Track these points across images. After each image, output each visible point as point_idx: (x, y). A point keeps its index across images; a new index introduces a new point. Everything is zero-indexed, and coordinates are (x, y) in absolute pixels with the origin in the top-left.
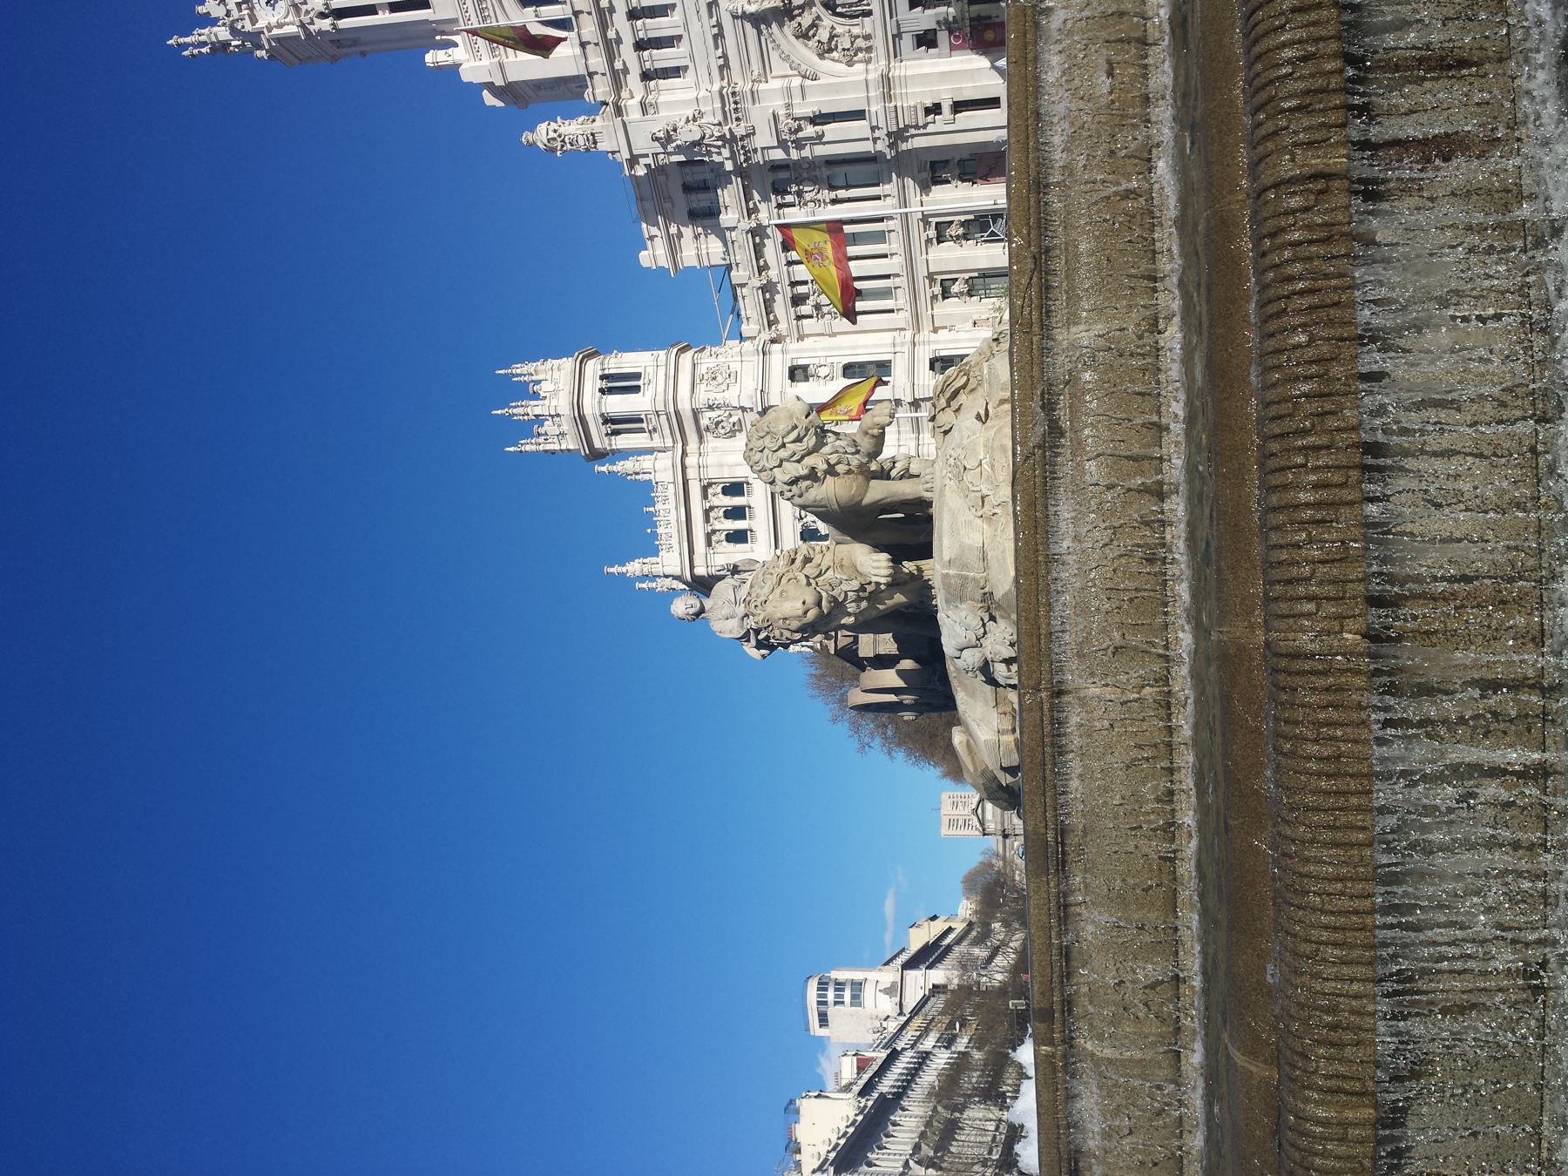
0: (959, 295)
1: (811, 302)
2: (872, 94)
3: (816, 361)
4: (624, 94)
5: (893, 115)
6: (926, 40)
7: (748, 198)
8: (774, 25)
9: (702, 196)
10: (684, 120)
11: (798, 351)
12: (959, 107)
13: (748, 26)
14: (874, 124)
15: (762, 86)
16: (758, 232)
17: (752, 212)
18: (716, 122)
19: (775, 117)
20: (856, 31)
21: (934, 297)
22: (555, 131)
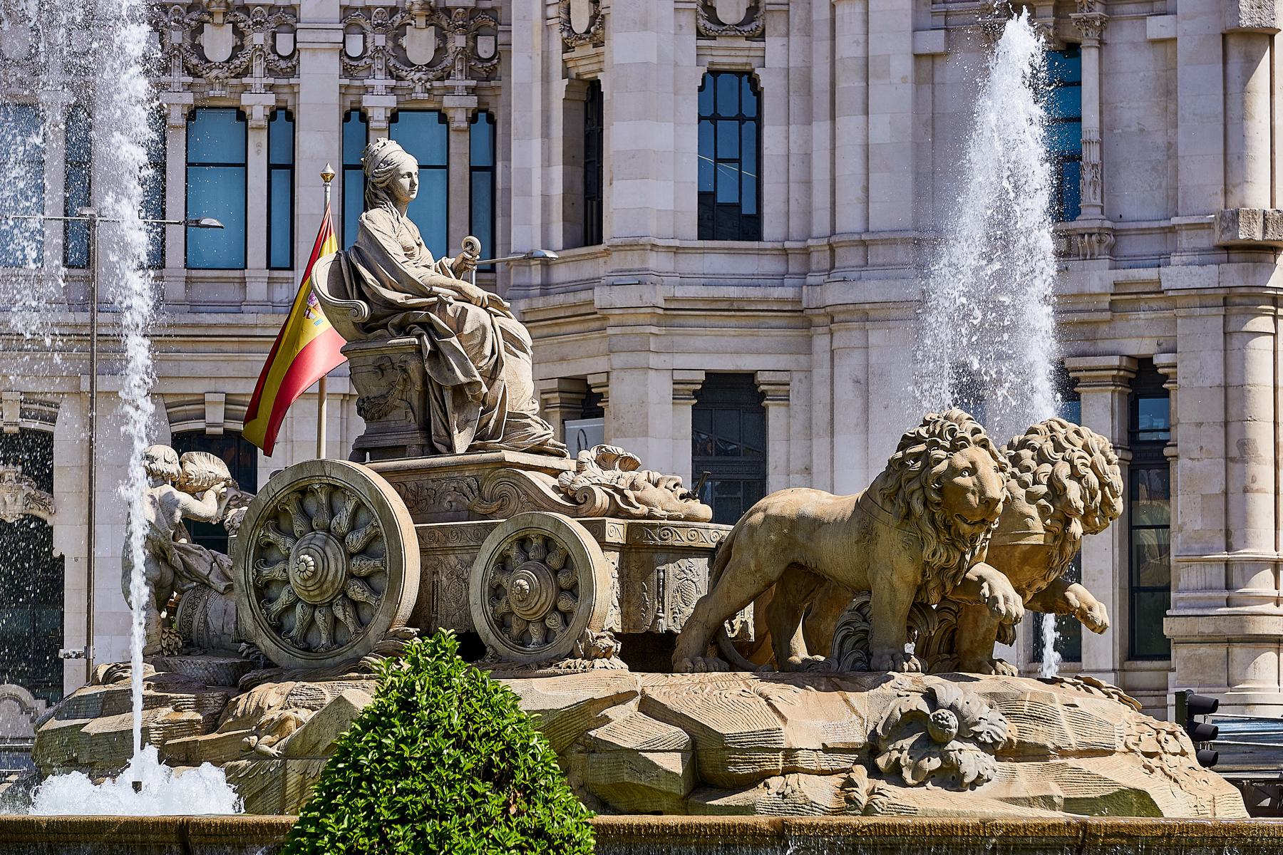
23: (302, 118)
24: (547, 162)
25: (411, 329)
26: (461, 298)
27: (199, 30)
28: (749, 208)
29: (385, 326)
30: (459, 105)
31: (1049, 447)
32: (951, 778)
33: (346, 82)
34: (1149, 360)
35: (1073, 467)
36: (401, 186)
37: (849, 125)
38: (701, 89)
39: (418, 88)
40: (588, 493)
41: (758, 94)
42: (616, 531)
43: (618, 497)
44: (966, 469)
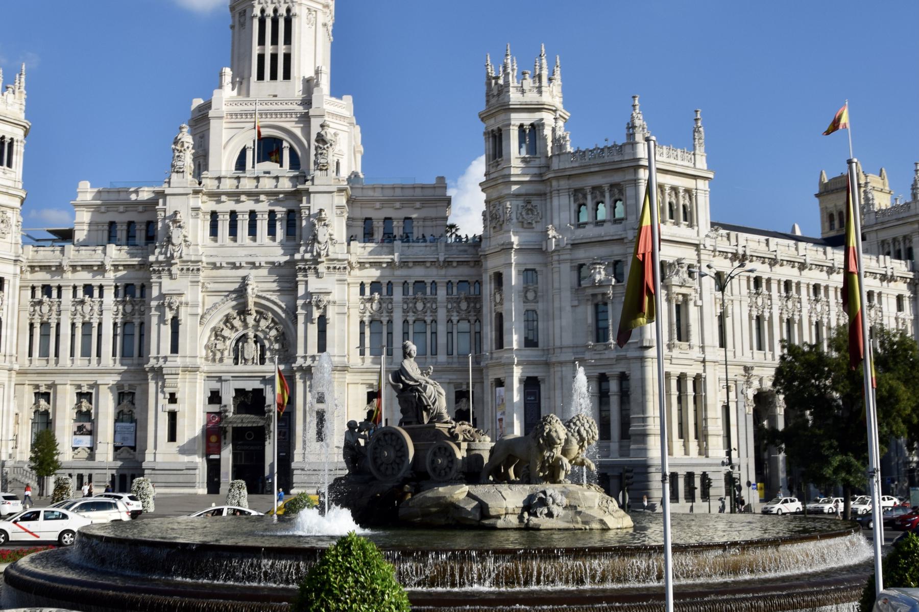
0: (37, 403)
1: (45, 298)
2: (188, 359)
3: (5, 298)
4: (205, 198)
5: (173, 372)
6: (215, 397)
7: (126, 267)
8: (234, 303)
9: (124, 234)
10: (186, 234)
11: (14, 285)
12: (173, 416)
13: (237, 286)
14: (169, 359)
15: (200, 288)
16: (101, 269)
17: (116, 267)
18: (183, 255)
19: (181, 295)
20: (226, 353)
21: (37, 387)
22: (188, 148)
23: (438, 322)
24: (491, 331)
27: (415, 303)
28: (535, 340)
30: (472, 319)
37: (557, 322)
41: (537, 315)
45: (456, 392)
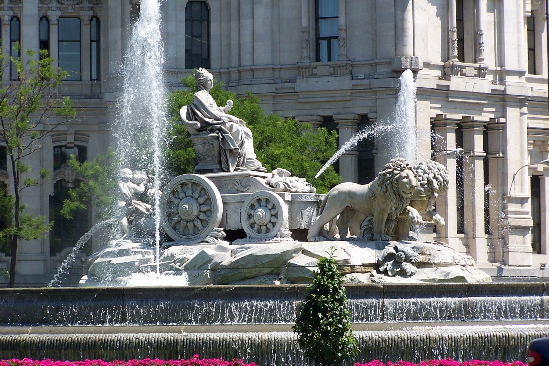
25: (215, 131)
26: (230, 120)
29: (206, 130)
31: (427, 169)
32: (403, 273)
33: (41, 5)
34: (366, 115)
35: (435, 175)
36: (209, 84)
37: (246, 23)
38: (186, 8)
39: (70, 8)
40: (277, 184)
41: (208, 10)
42: (288, 197)
43: (286, 186)
44: (405, 177)
45: (55, 147)
